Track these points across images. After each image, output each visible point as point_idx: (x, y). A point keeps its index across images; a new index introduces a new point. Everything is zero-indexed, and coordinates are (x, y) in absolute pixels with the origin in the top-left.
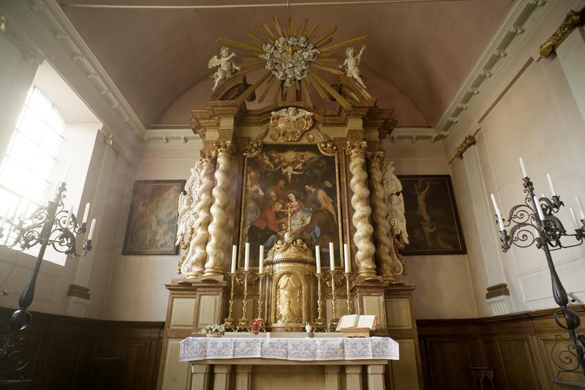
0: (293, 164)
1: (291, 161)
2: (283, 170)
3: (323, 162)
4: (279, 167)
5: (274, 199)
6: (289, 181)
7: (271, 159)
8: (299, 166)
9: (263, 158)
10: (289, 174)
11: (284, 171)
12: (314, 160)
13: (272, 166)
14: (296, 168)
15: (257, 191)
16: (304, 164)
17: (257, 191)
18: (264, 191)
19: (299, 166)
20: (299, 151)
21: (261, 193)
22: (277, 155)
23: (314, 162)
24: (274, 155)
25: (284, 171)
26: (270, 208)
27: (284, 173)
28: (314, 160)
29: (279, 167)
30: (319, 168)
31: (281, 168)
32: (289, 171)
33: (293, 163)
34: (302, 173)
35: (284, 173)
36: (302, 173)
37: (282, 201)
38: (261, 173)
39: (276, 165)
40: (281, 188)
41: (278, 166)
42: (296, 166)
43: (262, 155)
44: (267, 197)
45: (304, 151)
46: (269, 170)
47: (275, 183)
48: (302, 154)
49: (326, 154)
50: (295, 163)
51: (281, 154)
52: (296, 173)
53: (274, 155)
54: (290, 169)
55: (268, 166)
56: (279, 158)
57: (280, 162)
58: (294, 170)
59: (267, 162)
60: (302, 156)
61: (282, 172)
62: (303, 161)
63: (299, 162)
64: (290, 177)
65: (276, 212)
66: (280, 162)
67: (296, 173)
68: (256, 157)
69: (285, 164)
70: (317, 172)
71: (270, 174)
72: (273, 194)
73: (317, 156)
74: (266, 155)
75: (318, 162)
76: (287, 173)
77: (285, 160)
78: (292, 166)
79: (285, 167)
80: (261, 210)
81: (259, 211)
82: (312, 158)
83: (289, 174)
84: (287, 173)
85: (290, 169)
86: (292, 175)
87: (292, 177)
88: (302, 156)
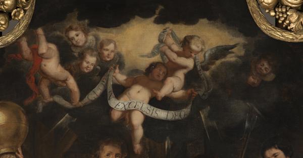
0: (150, 76)
1: (144, 63)
2: (113, 102)
3: (265, 66)
4: (98, 91)
6: (138, 147)
7: (68, 56)
8: (173, 86)
9: (35, 51)
10: (137, 119)
11: (118, 105)
12: (230, 58)
13: (72, 83)
14: (165, 91)
16: (192, 78)
19: (173, 86)
20: (175, 21)
22: (91, 38)
23: (231, 65)
24: (78, 37)
25: (118, 105)
27: (116, 115)
28: (230, 58)
29: (98, 91)
30: (248, 92)
31: (104, 97)
32: (136, 104)
33: (153, 66)
34: (185, 112)
35: (116, 115)
36: (185, 112)
39: (86, 82)
41: (94, 85)
42: (162, 82)
43: (32, 40)
45: (190, 20)
46: (58, 99)
48: (182, 31)
49: (278, 35)
50: (159, 72)
51: (103, 34)
52: (162, 114)
53: (78, 37)
54: (139, 96)
55: (56, 86)
56: (98, 49)
57: (103, 69)
58: (154, 102)
59: (53, 66)
60: (186, 43)
61: (110, 109)
62: (189, 63)
63: (171, 69)
64: (139, 133)
66: (103, 69)
67: (162, 114)
68: (14, 47)
69: (121, 78)
70: (240, 108)
71: (64, 119)
73: (241, 40)
74: (49, 40)
75: (244, 66)
76: (128, 113)
77: (119, 62)
78: (145, 85)
79: (120, 90)
82: (223, 51)
83: (137, 119)
84: (128, 113)
85: (139, 96)
86: (148, 122)
87: (146, 134)
88: (186, 43)
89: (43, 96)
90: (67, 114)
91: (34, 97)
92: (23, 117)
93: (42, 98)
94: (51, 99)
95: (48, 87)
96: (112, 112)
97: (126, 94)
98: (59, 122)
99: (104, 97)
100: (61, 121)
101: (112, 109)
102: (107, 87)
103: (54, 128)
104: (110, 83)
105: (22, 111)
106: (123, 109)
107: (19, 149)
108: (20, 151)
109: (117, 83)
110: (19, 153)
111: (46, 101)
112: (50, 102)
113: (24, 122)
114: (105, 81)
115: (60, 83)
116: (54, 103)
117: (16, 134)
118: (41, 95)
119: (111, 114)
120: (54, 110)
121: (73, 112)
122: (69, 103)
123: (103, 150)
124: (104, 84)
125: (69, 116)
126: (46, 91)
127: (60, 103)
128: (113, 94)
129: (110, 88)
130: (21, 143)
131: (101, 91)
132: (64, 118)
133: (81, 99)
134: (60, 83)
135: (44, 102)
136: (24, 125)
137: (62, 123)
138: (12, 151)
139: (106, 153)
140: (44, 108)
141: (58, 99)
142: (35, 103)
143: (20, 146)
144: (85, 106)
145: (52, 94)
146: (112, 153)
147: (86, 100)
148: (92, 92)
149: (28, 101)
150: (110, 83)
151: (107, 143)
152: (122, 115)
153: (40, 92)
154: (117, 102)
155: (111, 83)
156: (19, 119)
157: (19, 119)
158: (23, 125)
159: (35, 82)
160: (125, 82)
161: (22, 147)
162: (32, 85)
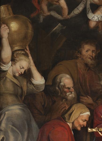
2: (90, 16)
4: (80, 8)
5: (71, 96)
15: (27, 75)
17: (27, 75)
18: (44, 74)
21: (38, 80)
26: (62, 118)
29: (80, 8)
31: (84, 13)
37: (89, 100)
38: (34, 22)
40: (86, 65)
44: (52, 90)
46: (53, 13)
47: (72, 51)
61: (88, 20)
65: (75, 130)
71: (57, 27)
72: (66, 81)
80: (41, 125)
81: (34, 125)
89: (43, 11)
90: (60, 24)
91: (37, 12)
92: (30, 26)
93: (43, 13)
94: (49, 14)
95: (47, 5)
96: (90, 22)
97: (99, 10)
98: (54, 29)
99: (84, 13)
100: (56, 28)
101: (90, 20)
102: (86, 6)
103: (51, 33)
104: (89, 3)
105: (29, 22)
106: (97, 20)
107: (27, 47)
108: (28, 49)
109: (94, 3)
110: (27, 50)
111: (45, 15)
112: (48, 16)
113: (30, 29)
114: (85, 1)
115: (55, 2)
116: (51, 16)
117: (25, 37)
118: (42, 11)
119: (89, 23)
120: (51, 21)
121: (64, 22)
122: (60, 16)
123: (83, 48)
124: (84, 3)
125: (61, 25)
126: (45, 8)
127: (55, 16)
128: (90, 10)
129: (88, 6)
130: (29, 43)
131: (83, 8)
132: (58, 26)
133: (69, 13)
134: (55, 2)
135: (44, 15)
136: (30, 31)
137: (56, 30)
138: (22, 49)
139: (86, 50)
140: (44, 19)
141: (53, 13)
142: (38, 16)
143: (27, 45)
144: (72, 18)
145: (49, 10)
146: (89, 50)
147: (72, 14)
148: (76, 9)
149: (34, 15)
150: (89, 3)
151: (87, 43)
152: (97, 24)
153: (42, 9)
154: (93, 15)
155: (89, 3)
156: (27, 27)
157: (27, 27)
158: (30, 31)
159: (38, 2)
160: (98, 2)
161: (29, 46)
162: (36, 4)
